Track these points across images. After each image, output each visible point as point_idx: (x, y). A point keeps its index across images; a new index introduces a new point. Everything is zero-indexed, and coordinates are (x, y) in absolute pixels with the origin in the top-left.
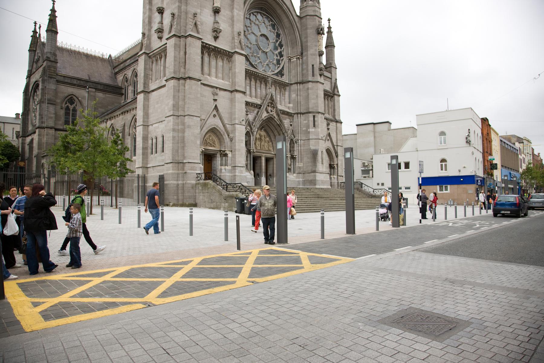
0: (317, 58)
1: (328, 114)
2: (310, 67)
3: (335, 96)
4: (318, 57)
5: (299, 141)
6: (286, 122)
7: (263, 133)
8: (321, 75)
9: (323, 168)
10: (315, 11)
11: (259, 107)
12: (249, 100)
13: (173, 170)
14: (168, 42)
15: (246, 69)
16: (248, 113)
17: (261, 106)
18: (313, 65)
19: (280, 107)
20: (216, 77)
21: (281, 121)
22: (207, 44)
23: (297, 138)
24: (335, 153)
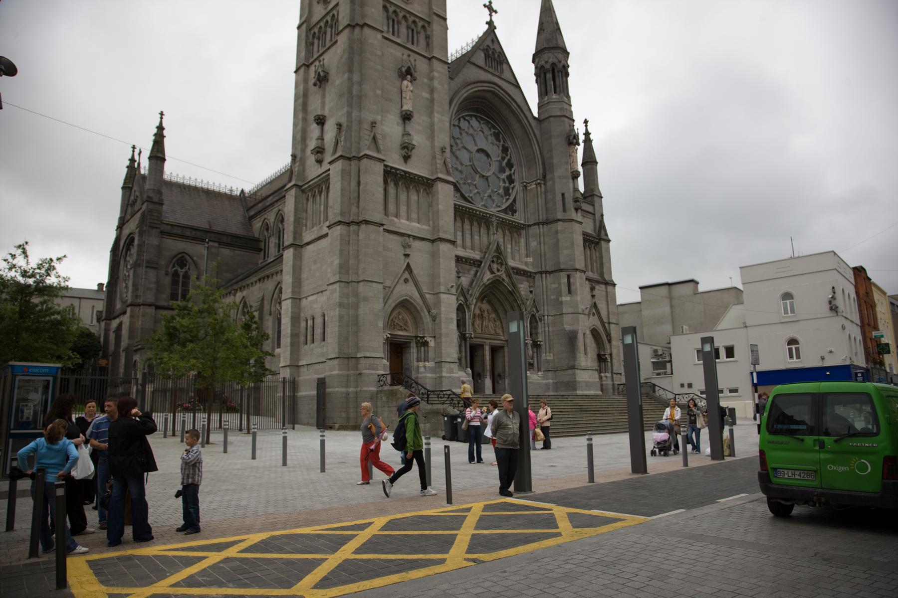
1: (592, 272)
2: (559, 197)
3: (602, 242)
4: (571, 181)
5: (546, 317)
6: (523, 287)
7: (485, 306)
8: (576, 210)
9: (587, 361)
10: (562, 109)
11: (477, 264)
12: (461, 252)
13: (339, 369)
14: (331, 167)
15: (455, 205)
16: (461, 275)
17: (481, 262)
18: (563, 195)
19: (512, 263)
20: (408, 219)
21: (514, 286)
22: (392, 168)
23: (542, 312)
24: (607, 336)
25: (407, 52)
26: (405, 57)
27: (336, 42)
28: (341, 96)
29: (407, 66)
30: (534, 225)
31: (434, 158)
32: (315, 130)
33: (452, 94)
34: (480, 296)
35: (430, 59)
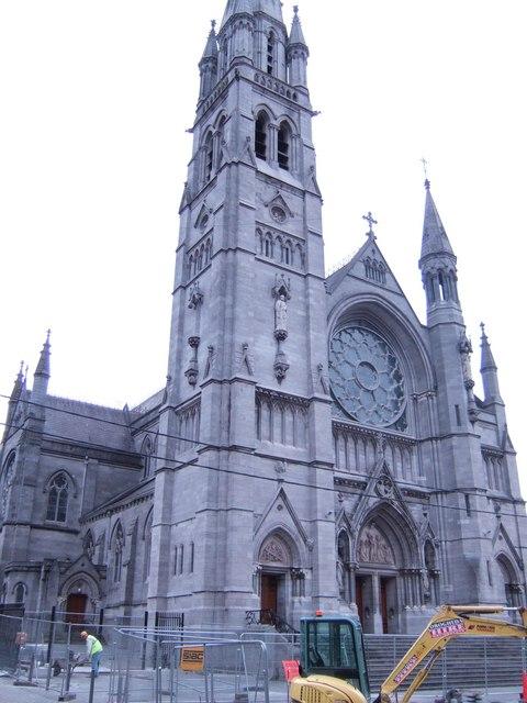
0: (462, 393)
2: (452, 410)
4: (465, 391)
6: (416, 511)
7: (374, 532)
8: (473, 422)
9: (492, 593)
13: (205, 605)
15: (333, 422)
17: (366, 484)
18: (457, 406)
20: (283, 441)
21: (405, 509)
22: (264, 390)
25: (281, 272)
26: (279, 276)
28: (214, 318)
30: (427, 440)
31: (310, 376)
32: (189, 352)
33: (330, 308)
34: (366, 520)
35: (305, 277)
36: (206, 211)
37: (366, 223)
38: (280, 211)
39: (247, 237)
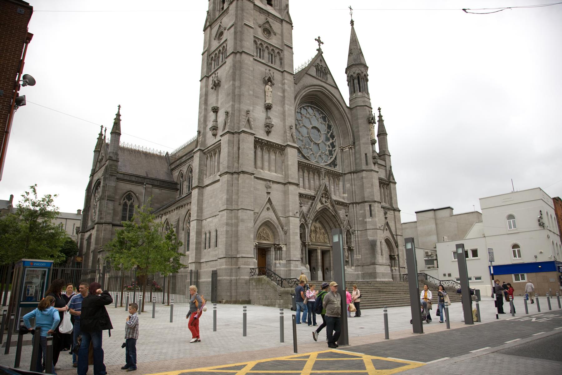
0: (370, 147)
3: (391, 184)
4: (371, 146)
5: (356, 231)
6: (342, 213)
7: (318, 225)
8: (374, 164)
10: (364, 101)
11: (313, 198)
13: (226, 265)
14: (222, 138)
15: (298, 161)
16: (302, 205)
17: (315, 197)
18: (366, 154)
19: (334, 198)
21: (336, 212)
22: (259, 139)
23: (354, 228)
24: (395, 243)
26: (267, 71)
27: (225, 62)
28: (228, 95)
29: (269, 76)
30: (348, 173)
31: (285, 132)
32: (212, 116)
33: (296, 93)
34: (314, 218)
35: (282, 72)
36: (222, 29)
37: (317, 43)
38: (268, 31)
39: (249, 45)
